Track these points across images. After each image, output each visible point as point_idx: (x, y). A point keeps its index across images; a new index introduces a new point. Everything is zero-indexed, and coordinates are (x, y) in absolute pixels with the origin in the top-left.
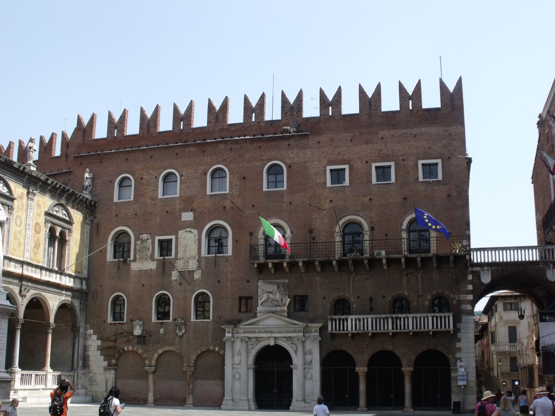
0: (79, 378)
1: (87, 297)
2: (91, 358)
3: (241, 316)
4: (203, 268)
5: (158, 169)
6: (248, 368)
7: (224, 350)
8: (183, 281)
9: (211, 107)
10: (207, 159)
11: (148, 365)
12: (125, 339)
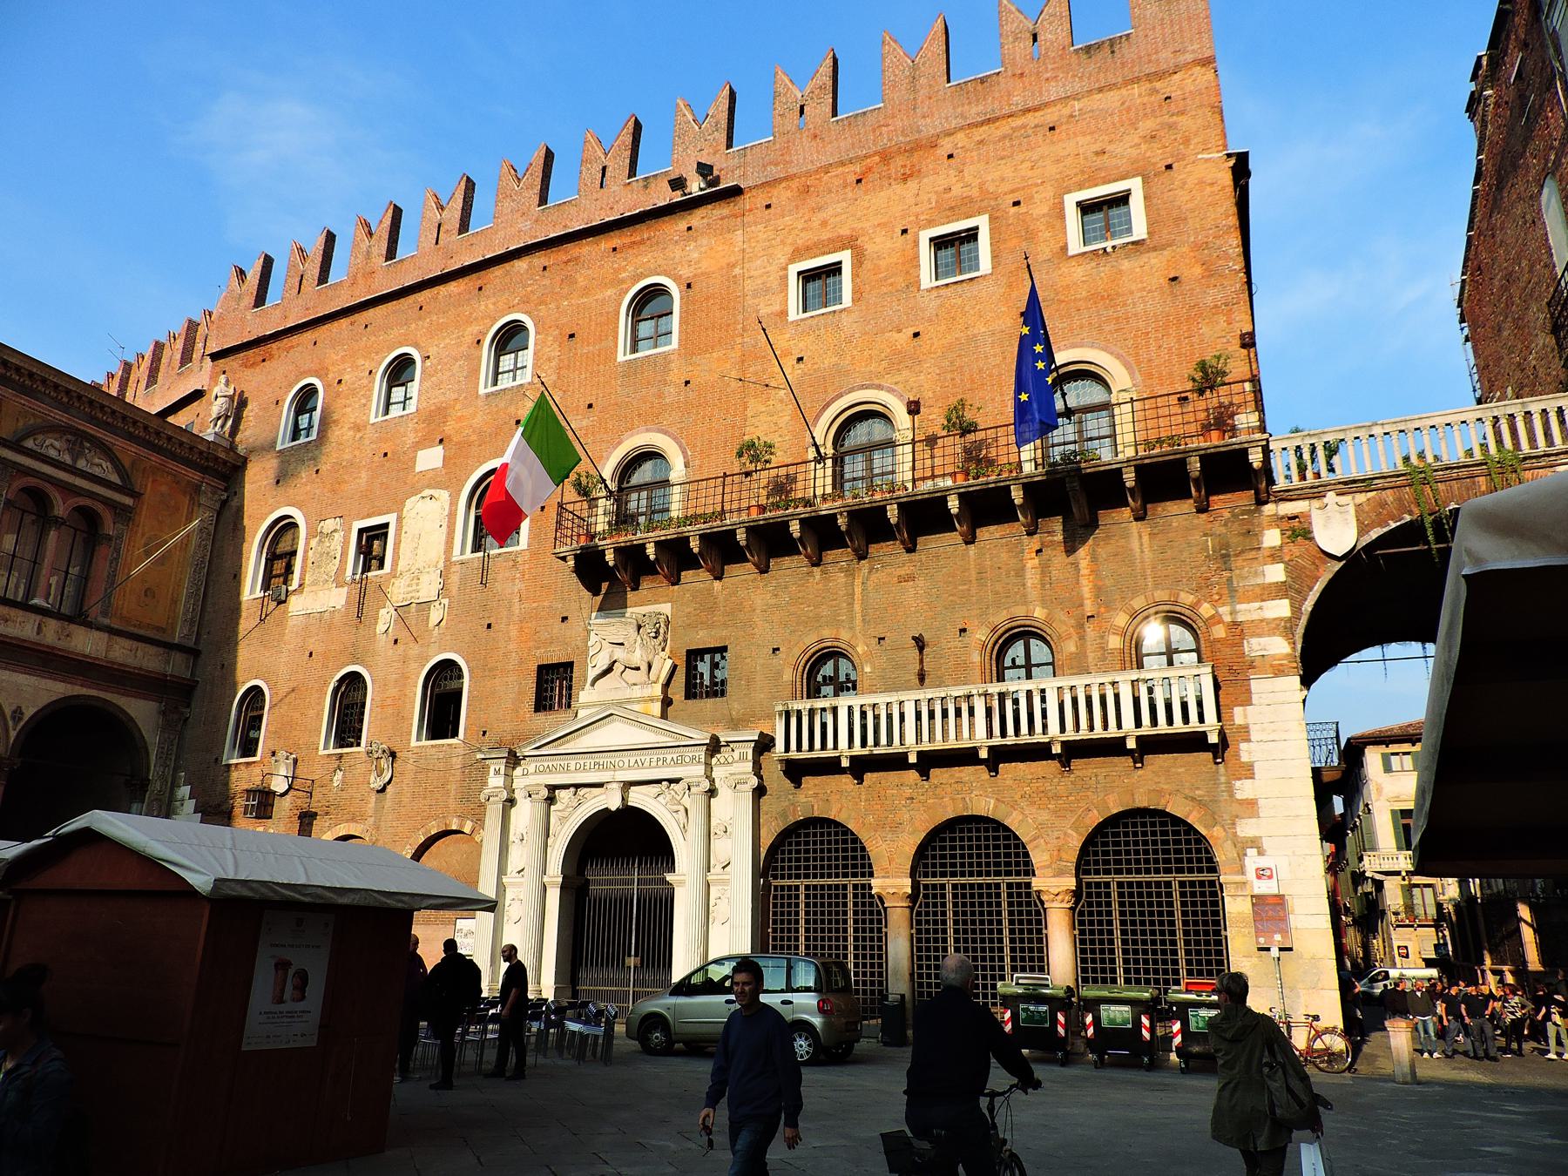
4: (454, 590)
8: (403, 635)
10: (485, 305)
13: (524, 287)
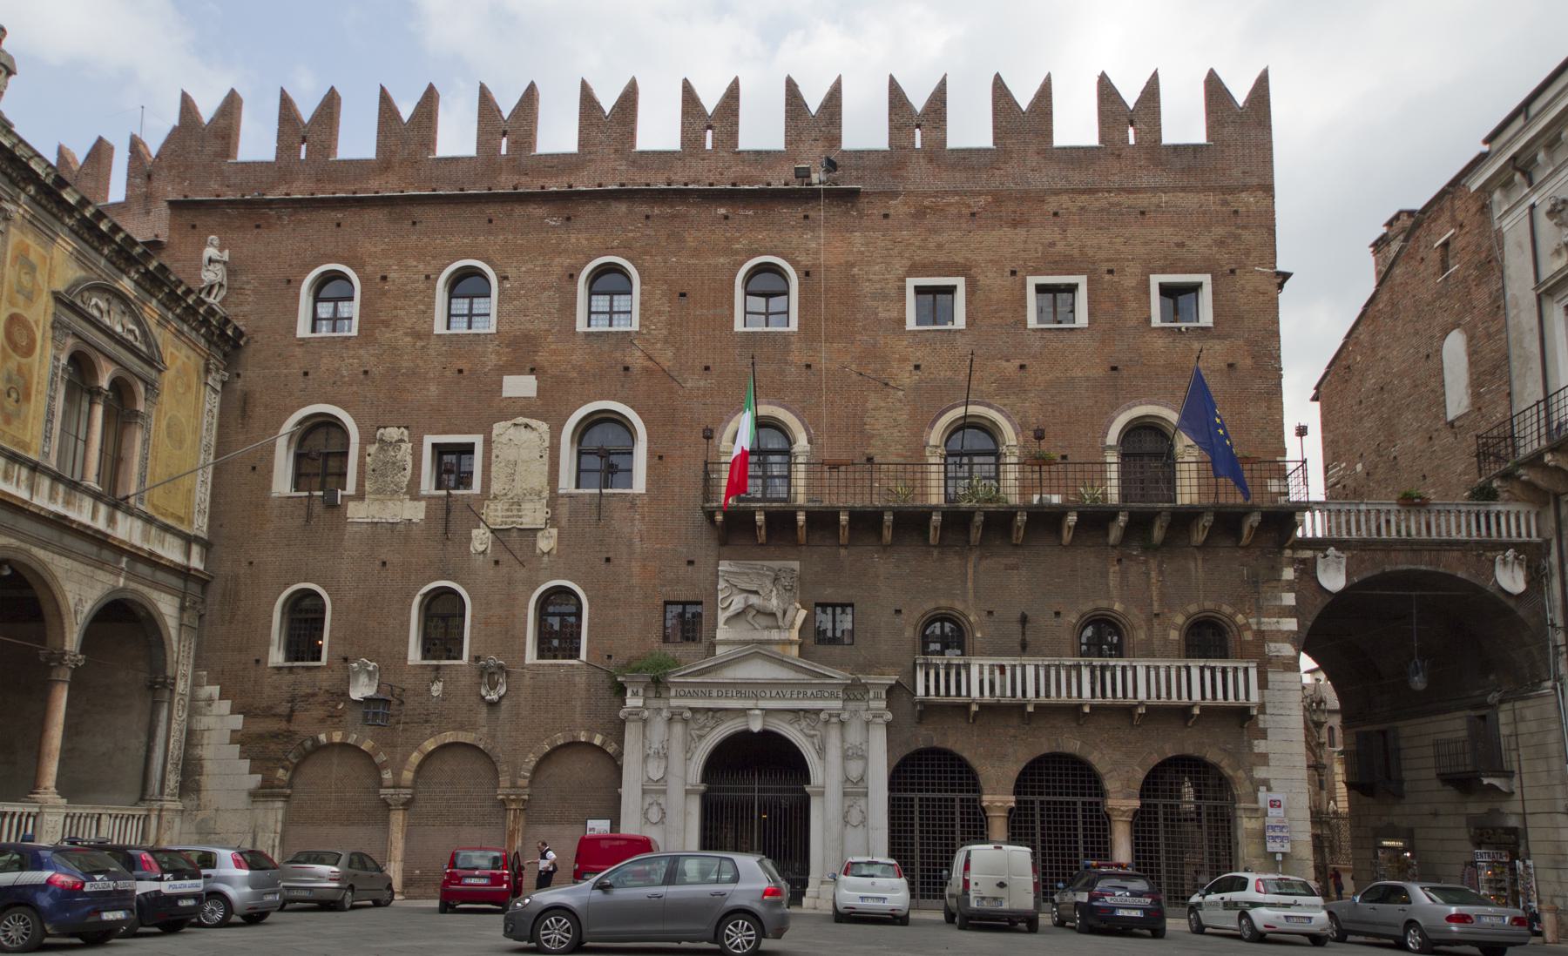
0: (164, 824)
1: (204, 591)
2: (208, 766)
3: (672, 650)
4: (564, 522)
5: (434, 258)
6: (687, 792)
7: (620, 742)
8: (505, 557)
9: (588, 100)
10: (577, 239)
11: (390, 783)
12: (319, 712)
13: (625, 231)
